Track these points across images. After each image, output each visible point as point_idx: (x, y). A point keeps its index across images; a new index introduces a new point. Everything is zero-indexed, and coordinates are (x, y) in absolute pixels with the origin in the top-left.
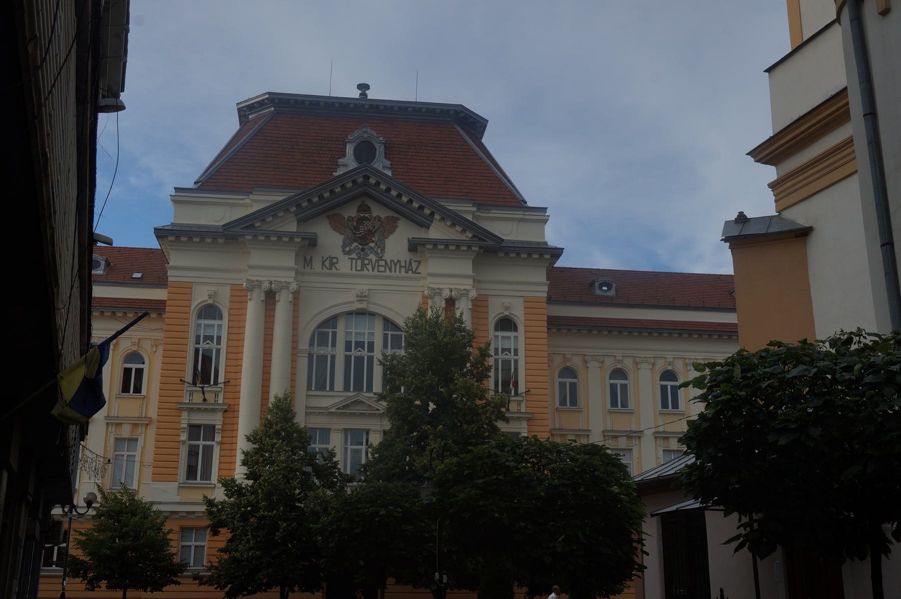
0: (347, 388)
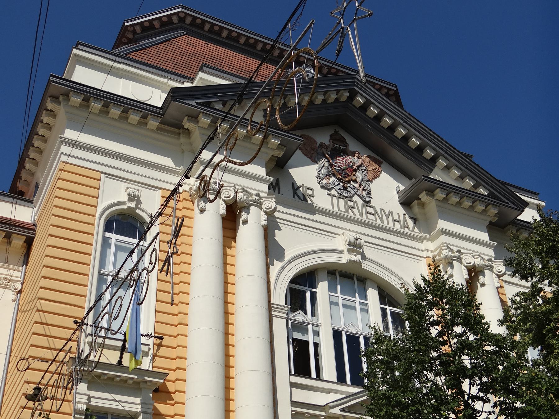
0: (341, 379)
